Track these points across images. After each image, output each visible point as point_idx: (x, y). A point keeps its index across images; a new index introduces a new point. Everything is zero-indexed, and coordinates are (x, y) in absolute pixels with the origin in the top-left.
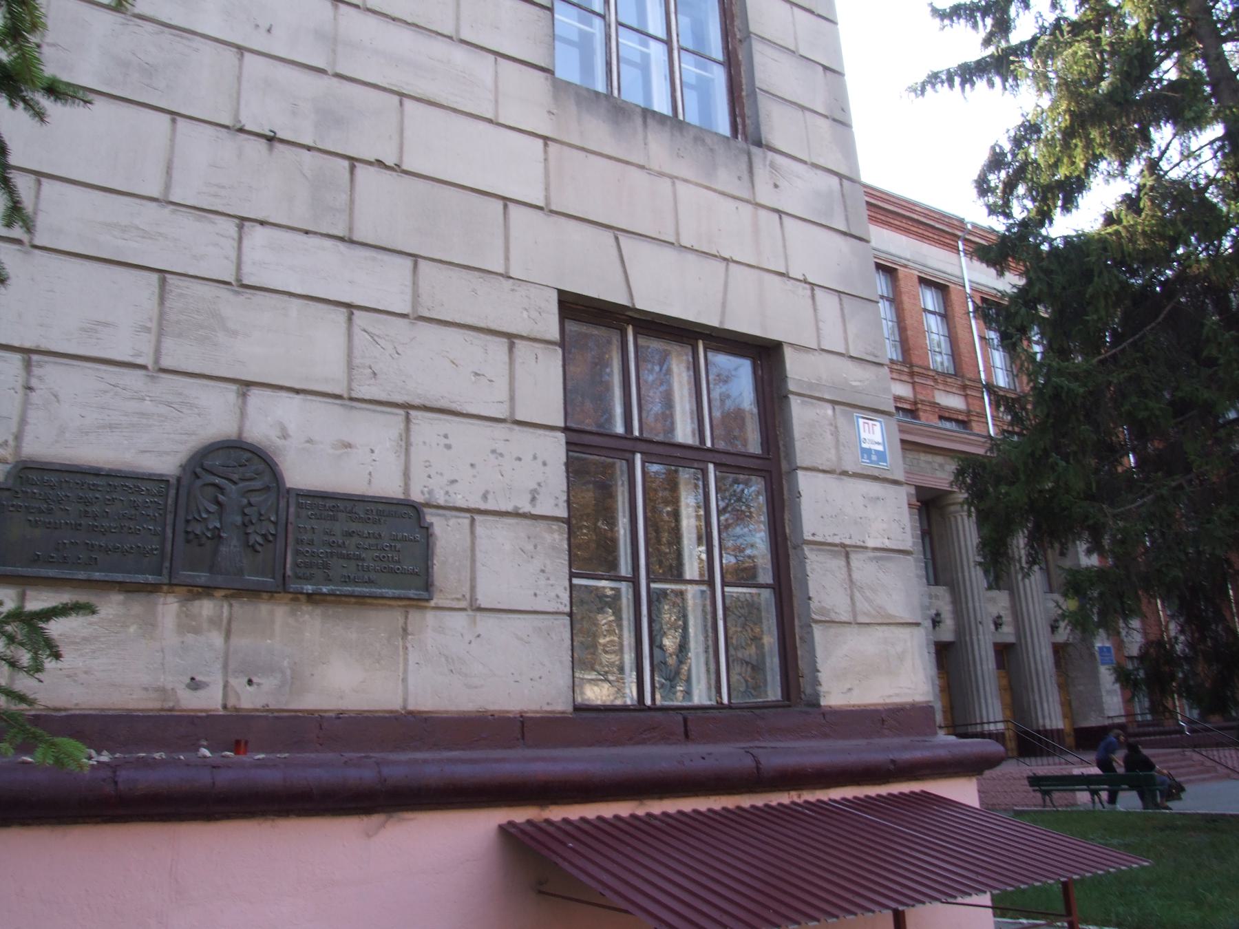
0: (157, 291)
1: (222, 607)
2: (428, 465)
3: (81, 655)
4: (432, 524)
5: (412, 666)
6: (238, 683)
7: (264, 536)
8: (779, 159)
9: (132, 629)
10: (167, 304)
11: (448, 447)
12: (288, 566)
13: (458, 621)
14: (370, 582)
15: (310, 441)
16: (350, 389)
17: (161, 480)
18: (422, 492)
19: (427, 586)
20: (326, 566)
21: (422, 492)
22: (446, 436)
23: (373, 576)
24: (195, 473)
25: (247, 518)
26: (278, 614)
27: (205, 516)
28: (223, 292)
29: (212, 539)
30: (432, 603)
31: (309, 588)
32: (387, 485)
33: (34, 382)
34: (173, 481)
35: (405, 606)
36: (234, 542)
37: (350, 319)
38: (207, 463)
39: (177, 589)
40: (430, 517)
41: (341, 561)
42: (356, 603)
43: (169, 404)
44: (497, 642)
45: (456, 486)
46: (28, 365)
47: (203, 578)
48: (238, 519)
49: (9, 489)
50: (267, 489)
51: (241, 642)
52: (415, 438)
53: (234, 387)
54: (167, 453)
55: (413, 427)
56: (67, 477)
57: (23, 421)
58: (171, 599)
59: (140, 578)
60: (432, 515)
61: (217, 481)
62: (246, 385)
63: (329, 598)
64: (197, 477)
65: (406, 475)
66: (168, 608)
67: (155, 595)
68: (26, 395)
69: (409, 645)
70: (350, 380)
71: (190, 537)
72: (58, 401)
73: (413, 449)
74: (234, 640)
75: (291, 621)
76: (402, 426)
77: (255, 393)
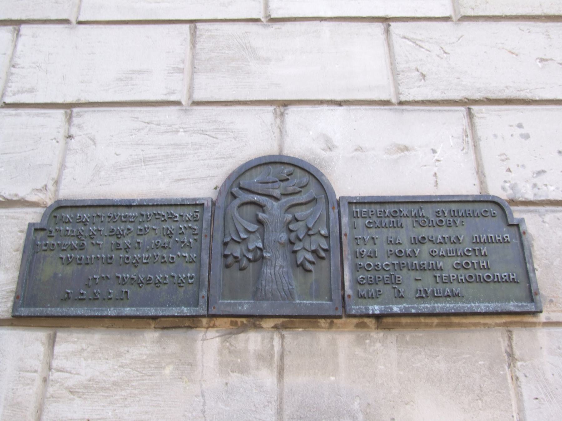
0: (188, 38)
1: (272, 339)
2: (505, 158)
3: (111, 403)
4: (523, 219)
5: (529, 404)
7: (314, 252)
9: (168, 371)
10: (198, 46)
11: (526, 136)
12: (347, 284)
14: (454, 295)
15: (359, 149)
16: (398, 93)
17: (196, 204)
18: (504, 188)
19: (531, 295)
20: (394, 281)
21: (504, 188)
22: (520, 126)
23: (457, 287)
24: (232, 194)
25: (293, 236)
26: (341, 344)
27: (243, 236)
29: (255, 261)
30: (542, 317)
31: (376, 309)
33: (74, 131)
34: (208, 204)
35: (505, 324)
36: (280, 262)
37: (387, 31)
38: (244, 182)
39: (218, 321)
40: (517, 213)
41: (413, 274)
42: (439, 325)
43: (203, 132)
45: (543, 177)
46: (69, 119)
47: (245, 307)
48: (284, 237)
49: (43, 229)
50: (313, 201)
51: (298, 381)
53: (271, 108)
54: (202, 179)
55: (476, 120)
56: (99, 212)
57: (63, 166)
58: (212, 333)
59: (174, 311)
60: (520, 211)
61: (256, 198)
63: (404, 320)
64: (234, 197)
65: (480, 172)
66: (209, 343)
67: (194, 331)
68: (67, 143)
69: (520, 375)
70: (396, 84)
71: (230, 262)
72: (95, 144)
73: (482, 144)
74: (288, 379)
75: (358, 351)
76: (465, 121)
77: (293, 112)
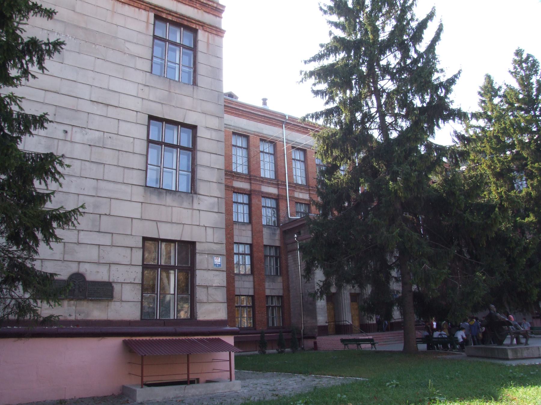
6: (78, 315)
8: (201, 196)
13: (118, 304)
17: (64, 281)
26: (85, 303)
28: (75, 245)
32: (105, 279)
40: (114, 285)
44: (126, 307)
46: (42, 262)
52: (111, 270)
62: (79, 262)
77: (81, 263)
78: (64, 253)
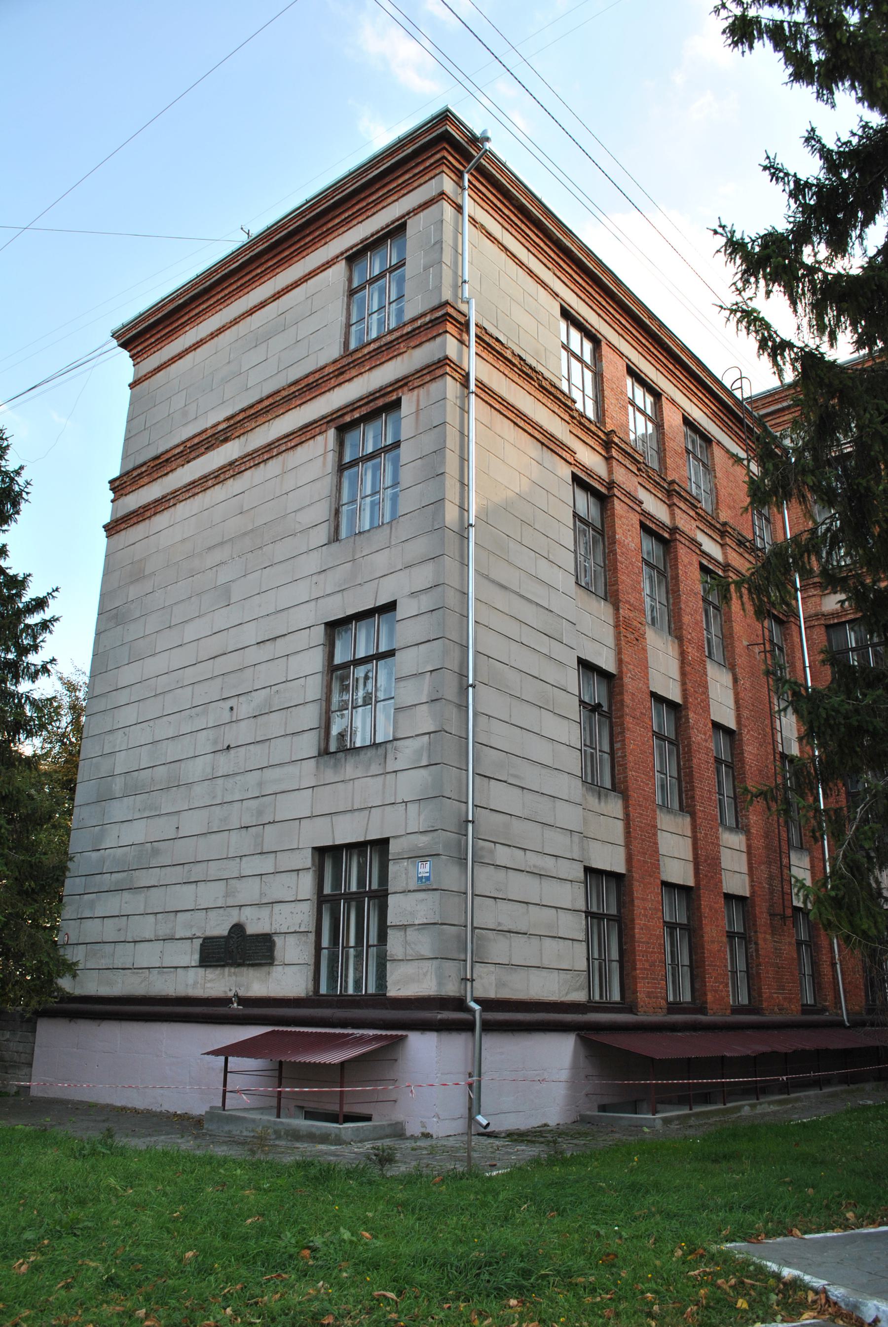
13: (280, 968)
26: (244, 970)
40: (276, 938)
66: (227, 969)
78: (227, 895)
